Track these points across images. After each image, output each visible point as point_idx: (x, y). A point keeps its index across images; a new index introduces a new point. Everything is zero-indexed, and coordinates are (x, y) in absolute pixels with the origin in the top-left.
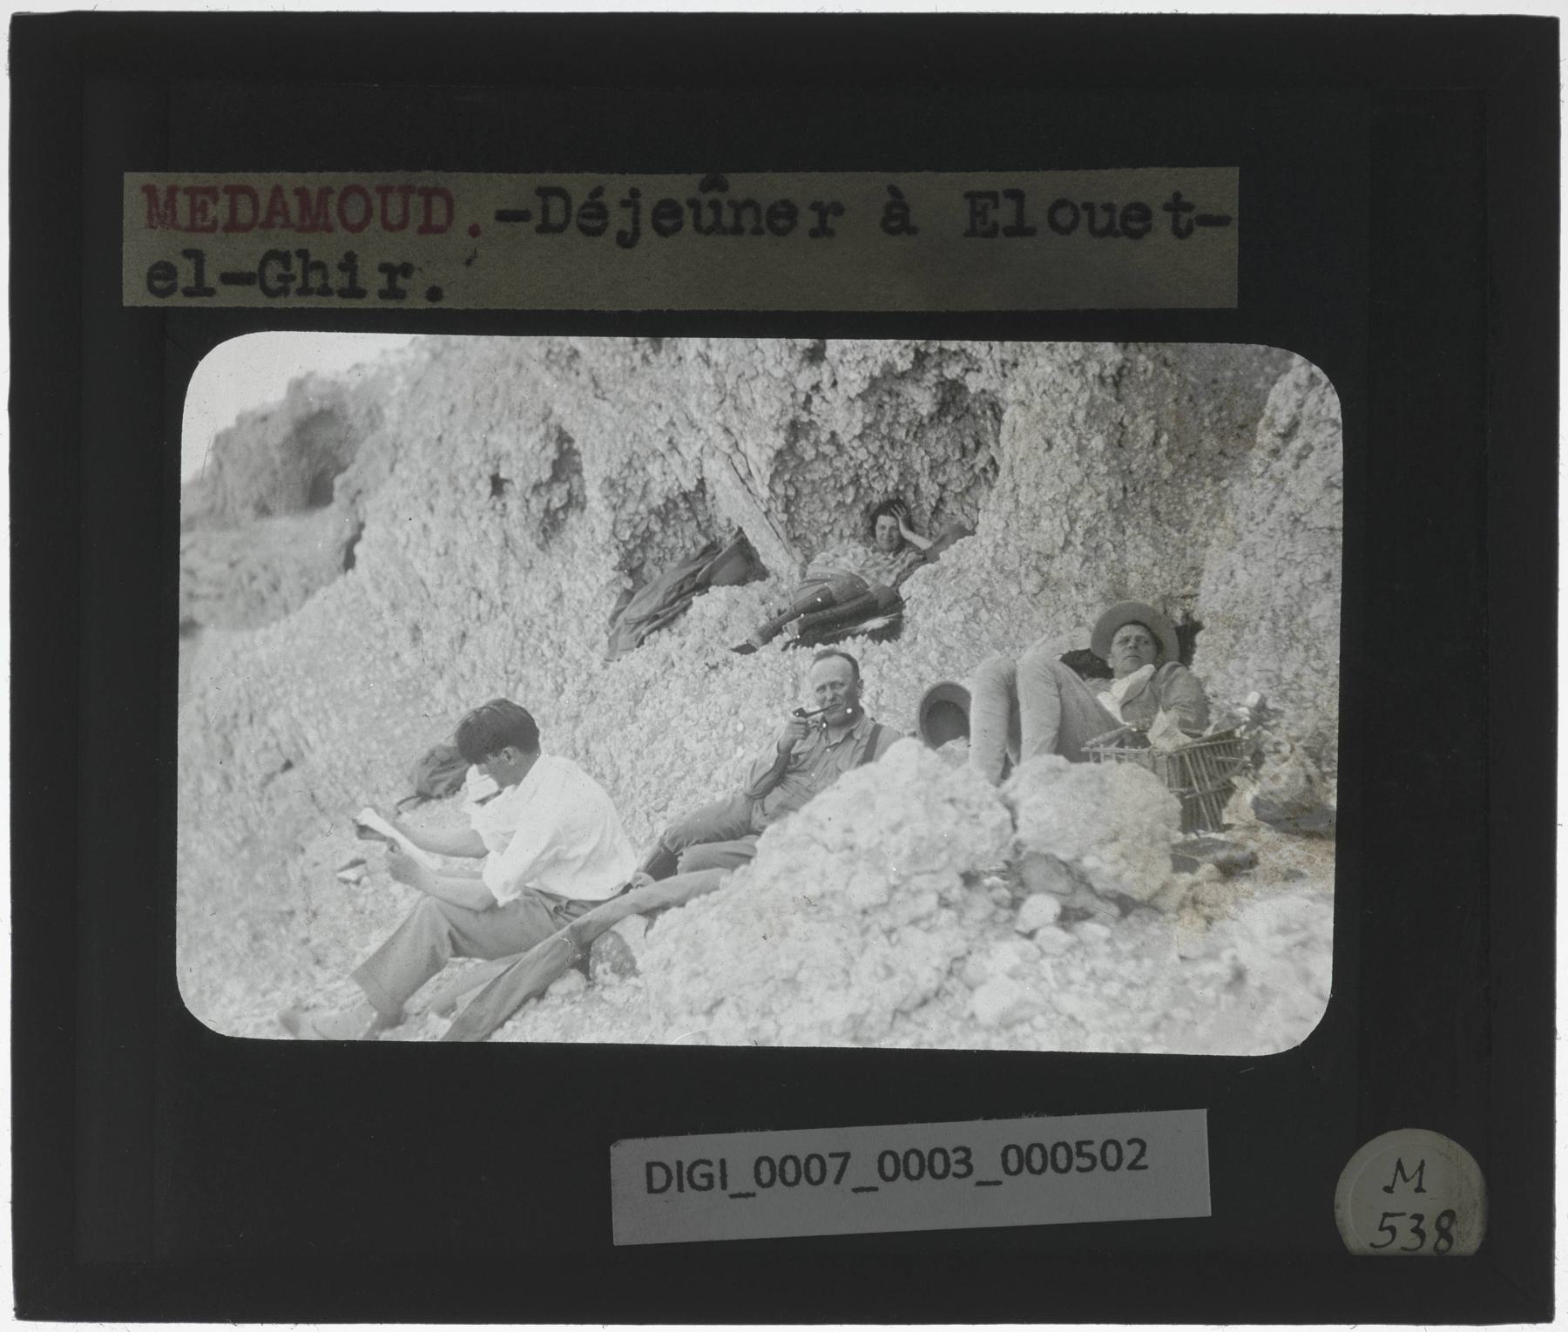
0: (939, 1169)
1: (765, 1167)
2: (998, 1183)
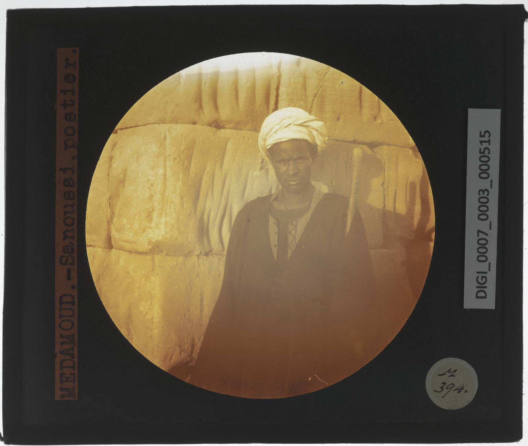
1: (480, 258)
2: (491, 181)
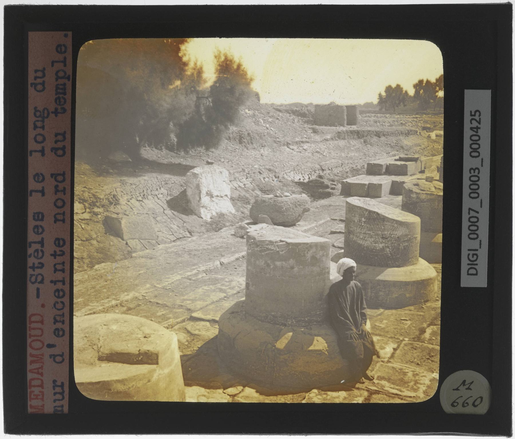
0: (476, 179)
